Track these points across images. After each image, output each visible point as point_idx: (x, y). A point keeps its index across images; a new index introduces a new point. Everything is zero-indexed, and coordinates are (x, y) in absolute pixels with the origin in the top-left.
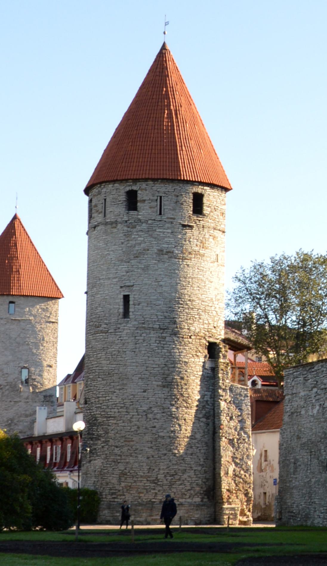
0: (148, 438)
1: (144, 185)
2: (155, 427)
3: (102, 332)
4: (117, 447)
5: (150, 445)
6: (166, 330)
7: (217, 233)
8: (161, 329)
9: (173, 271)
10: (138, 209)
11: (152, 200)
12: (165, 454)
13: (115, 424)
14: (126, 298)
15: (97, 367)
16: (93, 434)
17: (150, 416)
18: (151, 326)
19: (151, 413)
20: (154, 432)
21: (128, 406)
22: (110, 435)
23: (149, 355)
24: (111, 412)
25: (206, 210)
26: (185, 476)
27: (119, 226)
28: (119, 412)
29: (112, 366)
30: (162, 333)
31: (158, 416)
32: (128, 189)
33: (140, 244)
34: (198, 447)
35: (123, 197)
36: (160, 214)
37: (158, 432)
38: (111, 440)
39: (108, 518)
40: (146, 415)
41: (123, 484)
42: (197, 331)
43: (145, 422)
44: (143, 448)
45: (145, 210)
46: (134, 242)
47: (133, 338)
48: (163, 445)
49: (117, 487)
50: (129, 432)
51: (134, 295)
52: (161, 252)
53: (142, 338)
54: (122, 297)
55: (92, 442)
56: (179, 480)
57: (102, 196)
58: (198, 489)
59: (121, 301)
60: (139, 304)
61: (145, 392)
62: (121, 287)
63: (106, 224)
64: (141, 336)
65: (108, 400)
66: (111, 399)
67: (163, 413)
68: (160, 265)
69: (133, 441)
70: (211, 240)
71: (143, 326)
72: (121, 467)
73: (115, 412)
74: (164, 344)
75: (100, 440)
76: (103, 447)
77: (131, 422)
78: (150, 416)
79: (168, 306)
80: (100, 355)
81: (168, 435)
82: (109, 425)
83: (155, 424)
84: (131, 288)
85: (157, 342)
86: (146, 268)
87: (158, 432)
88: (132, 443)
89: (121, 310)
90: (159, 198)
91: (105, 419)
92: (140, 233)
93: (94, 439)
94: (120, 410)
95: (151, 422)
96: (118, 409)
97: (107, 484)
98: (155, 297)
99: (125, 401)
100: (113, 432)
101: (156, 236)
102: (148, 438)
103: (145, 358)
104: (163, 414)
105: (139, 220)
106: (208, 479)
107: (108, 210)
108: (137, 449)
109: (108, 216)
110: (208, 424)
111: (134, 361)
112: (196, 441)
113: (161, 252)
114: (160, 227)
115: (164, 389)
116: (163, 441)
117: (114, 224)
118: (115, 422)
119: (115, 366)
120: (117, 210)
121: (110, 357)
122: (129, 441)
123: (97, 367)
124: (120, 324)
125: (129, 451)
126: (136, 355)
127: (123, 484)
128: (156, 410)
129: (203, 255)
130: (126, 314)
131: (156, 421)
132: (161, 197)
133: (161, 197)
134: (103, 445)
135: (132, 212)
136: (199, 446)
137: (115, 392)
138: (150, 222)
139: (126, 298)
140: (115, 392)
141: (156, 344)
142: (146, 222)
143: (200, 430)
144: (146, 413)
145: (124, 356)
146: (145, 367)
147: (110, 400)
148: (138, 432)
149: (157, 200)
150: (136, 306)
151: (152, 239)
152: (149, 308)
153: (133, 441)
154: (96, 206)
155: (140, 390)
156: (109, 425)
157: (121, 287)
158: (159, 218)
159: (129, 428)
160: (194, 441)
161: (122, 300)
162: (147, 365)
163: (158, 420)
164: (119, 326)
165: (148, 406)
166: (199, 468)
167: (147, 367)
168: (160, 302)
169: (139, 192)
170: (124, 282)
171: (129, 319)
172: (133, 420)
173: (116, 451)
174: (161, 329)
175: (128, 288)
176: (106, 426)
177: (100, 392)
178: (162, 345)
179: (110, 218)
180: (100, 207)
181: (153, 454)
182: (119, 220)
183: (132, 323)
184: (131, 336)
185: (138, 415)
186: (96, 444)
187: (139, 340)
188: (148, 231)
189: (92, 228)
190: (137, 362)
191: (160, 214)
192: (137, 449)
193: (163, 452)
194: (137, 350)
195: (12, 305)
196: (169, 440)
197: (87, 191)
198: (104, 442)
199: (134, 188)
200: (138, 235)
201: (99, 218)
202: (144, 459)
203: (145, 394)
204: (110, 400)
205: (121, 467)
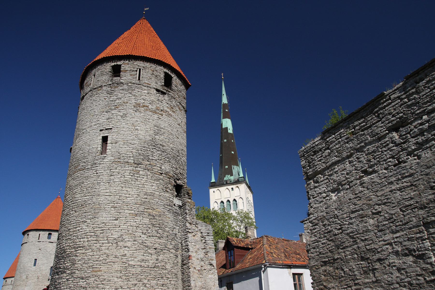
0: (117, 267)
2: (125, 255)
4: (82, 278)
5: (119, 275)
6: (140, 165)
8: (135, 164)
9: (148, 120)
10: (121, 76)
11: (133, 71)
12: (136, 285)
13: (83, 254)
15: (71, 202)
16: (60, 268)
17: (120, 244)
18: (126, 161)
19: (122, 241)
20: (124, 260)
21: (99, 234)
22: (76, 265)
23: (123, 185)
24: (80, 242)
27: (104, 88)
28: (88, 241)
29: (86, 197)
30: (136, 167)
31: (129, 244)
32: (113, 64)
34: (168, 278)
36: (139, 79)
37: (128, 261)
38: (77, 272)
40: (117, 243)
43: (115, 250)
44: (112, 278)
45: (125, 77)
47: (109, 171)
48: (133, 274)
50: (97, 261)
51: (112, 136)
52: (137, 106)
53: (117, 170)
54: (101, 138)
55: (57, 276)
60: (116, 143)
62: (101, 130)
64: (116, 169)
65: (78, 230)
66: (81, 229)
67: (135, 241)
68: (137, 114)
69: (101, 271)
71: (119, 160)
73: (84, 242)
74: (137, 177)
75: (65, 272)
76: (68, 280)
77: (100, 250)
78: (120, 244)
79: (143, 145)
80: (76, 190)
81: (139, 263)
82: (77, 256)
83: (126, 252)
84: (110, 131)
85: (131, 174)
86: (125, 116)
87: (128, 261)
88: (99, 273)
90: (138, 70)
91: (74, 250)
92: (121, 91)
93: (60, 273)
94: (90, 239)
95: (121, 251)
96: (87, 238)
98: (131, 138)
99: (95, 230)
100: (80, 262)
101: (135, 94)
102: (117, 267)
103: (119, 188)
104: (134, 242)
105: (122, 83)
108: (105, 280)
111: (108, 191)
112: (167, 272)
113: (137, 106)
115: (136, 218)
116: (133, 270)
118: (83, 251)
119: (88, 197)
121: (85, 189)
122: (96, 272)
123: (71, 202)
124: (97, 160)
125: (96, 283)
126: (110, 186)
128: (126, 237)
130: (104, 150)
131: (127, 249)
132: (140, 70)
133: (140, 70)
134: (68, 277)
135: (115, 78)
136: (169, 276)
137: (86, 222)
138: (129, 84)
140: (86, 222)
141: (130, 177)
143: (170, 261)
144: (116, 242)
145: (98, 187)
146: (118, 197)
147: (81, 230)
148: (107, 261)
149: (137, 71)
150: (114, 145)
151: (131, 95)
152: (126, 146)
153: (101, 271)
155: (112, 218)
156: (77, 256)
157: (101, 130)
159: (98, 257)
160: (164, 271)
161: (101, 141)
162: (121, 194)
163: (129, 248)
164: (96, 162)
165: (119, 234)
167: (120, 196)
168: (135, 142)
170: (104, 126)
171: (106, 155)
172: (103, 248)
173: (81, 283)
174: (135, 164)
175: (107, 131)
176: (74, 257)
177: (71, 224)
178: (136, 178)
181: (122, 284)
184: (106, 169)
185: (108, 243)
186: (61, 278)
187: (114, 172)
188: (129, 90)
190: (110, 192)
191: (139, 79)
192: (105, 280)
193: (133, 283)
194: (112, 181)
196: (139, 269)
199: (119, 63)
200: (119, 92)
203: (117, 222)
204: (81, 230)
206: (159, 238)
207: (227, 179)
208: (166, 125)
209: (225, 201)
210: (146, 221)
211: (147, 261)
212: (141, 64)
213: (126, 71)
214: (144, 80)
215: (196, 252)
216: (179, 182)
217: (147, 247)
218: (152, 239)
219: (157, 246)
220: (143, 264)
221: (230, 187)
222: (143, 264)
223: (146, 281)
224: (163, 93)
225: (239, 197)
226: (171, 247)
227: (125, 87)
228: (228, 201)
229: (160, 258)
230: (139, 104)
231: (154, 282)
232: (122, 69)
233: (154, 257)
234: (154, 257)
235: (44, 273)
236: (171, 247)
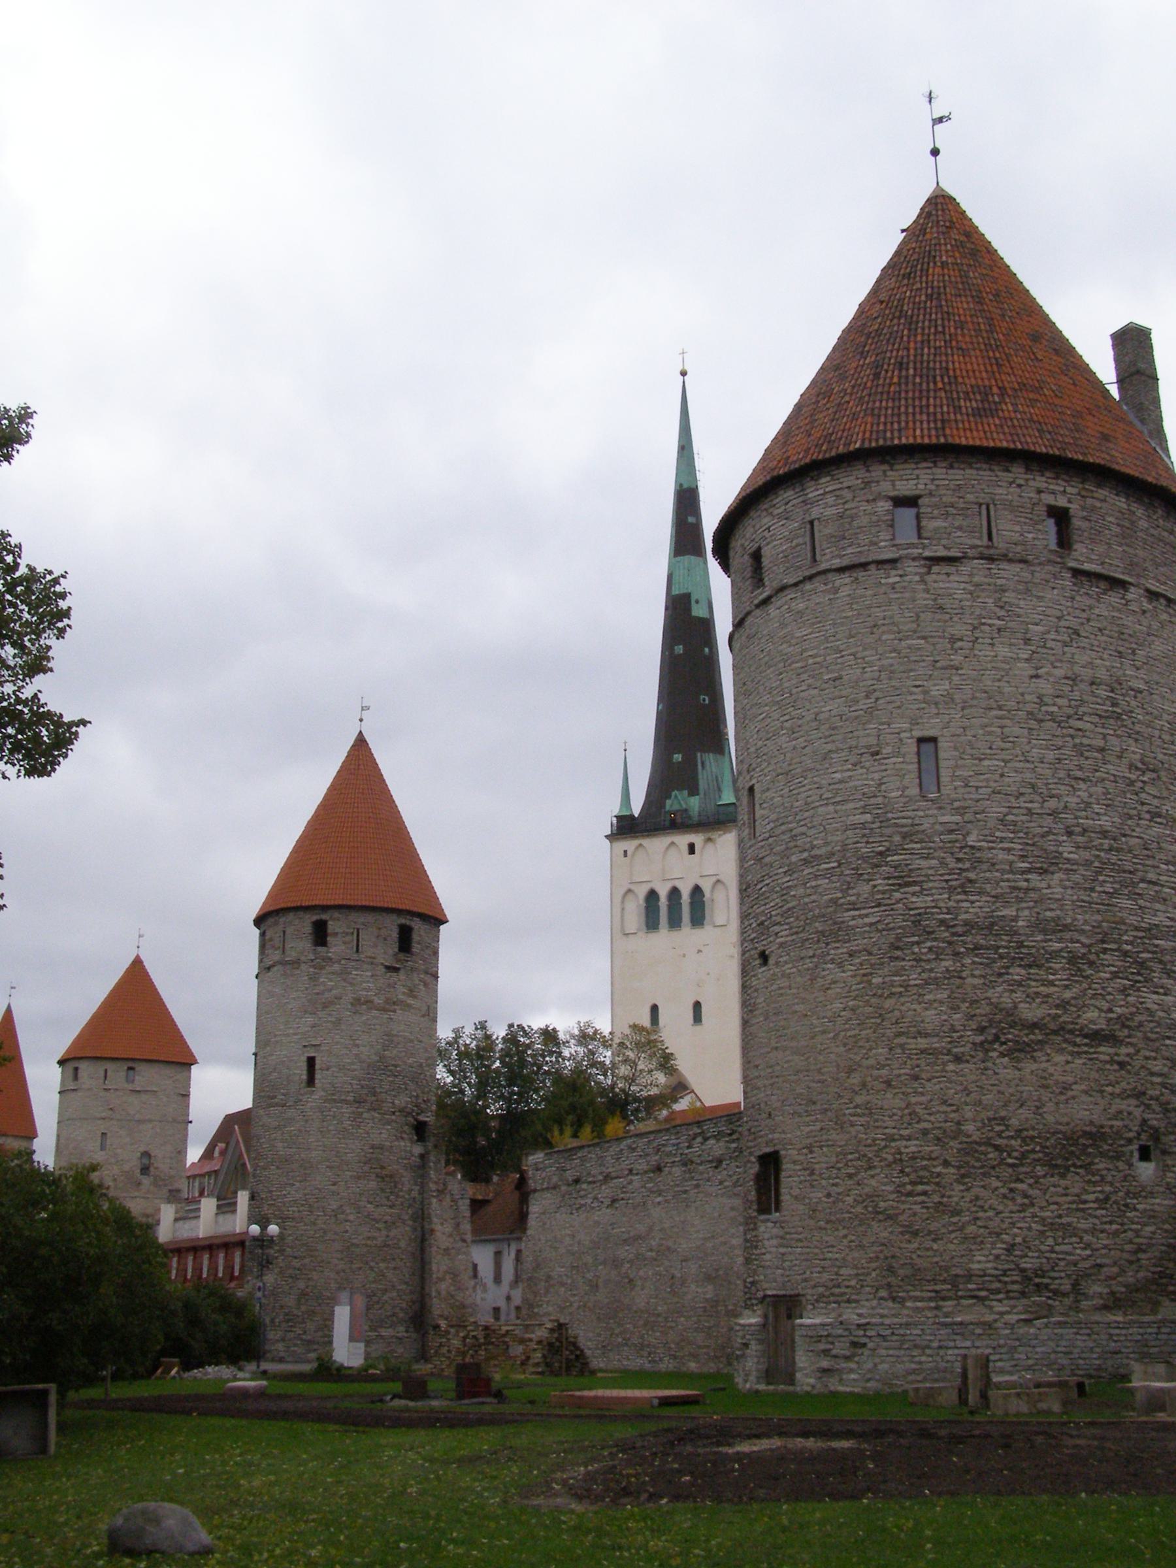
1: (336, 915)
3: (277, 1105)
4: (296, 1258)
5: (339, 1256)
7: (428, 979)
11: (347, 934)
14: (311, 1062)
17: (341, 1217)
19: (343, 1213)
25: (416, 948)
26: (385, 1297)
27: (303, 967)
31: (351, 1217)
32: (315, 918)
33: (330, 990)
35: (308, 929)
36: (357, 951)
39: (282, 1354)
41: (303, 1308)
42: (403, 1105)
45: (337, 947)
46: (322, 988)
49: (296, 1312)
52: (357, 1001)
54: (304, 1059)
56: (378, 1302)
57: (281, 927)
58: (401, 1315)
59: (303, 1065)
61: (334, 1184)
63: (283, 963)
70: (421, 987)
72: (301, 1284)
77: (315, 1224)
86: (339, 1021)
89: (305, 1077)
97: (282, 1307)
105: (331, 959)
106: (414, 1302)
107: (288, 946)
109: (288, 952)
110: (415, 1230)
113: (357, 1001)
114: (357, 969)
117: (296, 963)
120: (300, 944)
127: (303, 1308)
129: (409, 1006)
130: (311, 1081)
135: (320, 949)
139: (311, 1062)
142: (339, 962)
154: (271, 940)
158: (355, 956)
166: (404, 1287)
169: (330, 922)
179: (292, 955)
180: (277, 942)
182: (303, 958)
183: (318, 1094)
189: (265, 969)
195: (131, 1072)
197: (259, 921)
198: (278, 1251)
199: (324, 917)
201: (276, 956)
202: (332, 1275)
205: (301, 1284)
206: (391, 1207)
207: (676, 807)
208: (402, 1027)
209: (663, 893)
210: (373, 1184)
211: (374, 1238)
212: (361, 918)
213: (336, 934)
214: (367, 951)
215: (442, 1224)
216: (422, 1118)
217: (374, 1220)
218: (380, 1210)
219: (387, 1218)
220: (369, 1242)
221: (683, 840)
222: (369, 1242)
223: (372, 1264)
224: (396, 970)
225: (714, 879)
226: (406, 1217)
227: (336, 967)
228: (675, 893)
229: (392, 1234)
230: (359, 1000)
231: (382, 1265)
232: (330, 930)
233: (384, 1232)
234: (384, 1232)
235: (126, 1167)
236: (406, 1217)
